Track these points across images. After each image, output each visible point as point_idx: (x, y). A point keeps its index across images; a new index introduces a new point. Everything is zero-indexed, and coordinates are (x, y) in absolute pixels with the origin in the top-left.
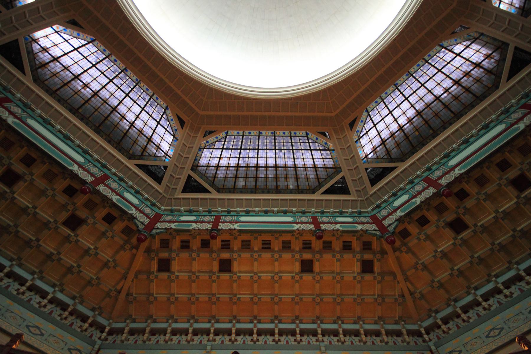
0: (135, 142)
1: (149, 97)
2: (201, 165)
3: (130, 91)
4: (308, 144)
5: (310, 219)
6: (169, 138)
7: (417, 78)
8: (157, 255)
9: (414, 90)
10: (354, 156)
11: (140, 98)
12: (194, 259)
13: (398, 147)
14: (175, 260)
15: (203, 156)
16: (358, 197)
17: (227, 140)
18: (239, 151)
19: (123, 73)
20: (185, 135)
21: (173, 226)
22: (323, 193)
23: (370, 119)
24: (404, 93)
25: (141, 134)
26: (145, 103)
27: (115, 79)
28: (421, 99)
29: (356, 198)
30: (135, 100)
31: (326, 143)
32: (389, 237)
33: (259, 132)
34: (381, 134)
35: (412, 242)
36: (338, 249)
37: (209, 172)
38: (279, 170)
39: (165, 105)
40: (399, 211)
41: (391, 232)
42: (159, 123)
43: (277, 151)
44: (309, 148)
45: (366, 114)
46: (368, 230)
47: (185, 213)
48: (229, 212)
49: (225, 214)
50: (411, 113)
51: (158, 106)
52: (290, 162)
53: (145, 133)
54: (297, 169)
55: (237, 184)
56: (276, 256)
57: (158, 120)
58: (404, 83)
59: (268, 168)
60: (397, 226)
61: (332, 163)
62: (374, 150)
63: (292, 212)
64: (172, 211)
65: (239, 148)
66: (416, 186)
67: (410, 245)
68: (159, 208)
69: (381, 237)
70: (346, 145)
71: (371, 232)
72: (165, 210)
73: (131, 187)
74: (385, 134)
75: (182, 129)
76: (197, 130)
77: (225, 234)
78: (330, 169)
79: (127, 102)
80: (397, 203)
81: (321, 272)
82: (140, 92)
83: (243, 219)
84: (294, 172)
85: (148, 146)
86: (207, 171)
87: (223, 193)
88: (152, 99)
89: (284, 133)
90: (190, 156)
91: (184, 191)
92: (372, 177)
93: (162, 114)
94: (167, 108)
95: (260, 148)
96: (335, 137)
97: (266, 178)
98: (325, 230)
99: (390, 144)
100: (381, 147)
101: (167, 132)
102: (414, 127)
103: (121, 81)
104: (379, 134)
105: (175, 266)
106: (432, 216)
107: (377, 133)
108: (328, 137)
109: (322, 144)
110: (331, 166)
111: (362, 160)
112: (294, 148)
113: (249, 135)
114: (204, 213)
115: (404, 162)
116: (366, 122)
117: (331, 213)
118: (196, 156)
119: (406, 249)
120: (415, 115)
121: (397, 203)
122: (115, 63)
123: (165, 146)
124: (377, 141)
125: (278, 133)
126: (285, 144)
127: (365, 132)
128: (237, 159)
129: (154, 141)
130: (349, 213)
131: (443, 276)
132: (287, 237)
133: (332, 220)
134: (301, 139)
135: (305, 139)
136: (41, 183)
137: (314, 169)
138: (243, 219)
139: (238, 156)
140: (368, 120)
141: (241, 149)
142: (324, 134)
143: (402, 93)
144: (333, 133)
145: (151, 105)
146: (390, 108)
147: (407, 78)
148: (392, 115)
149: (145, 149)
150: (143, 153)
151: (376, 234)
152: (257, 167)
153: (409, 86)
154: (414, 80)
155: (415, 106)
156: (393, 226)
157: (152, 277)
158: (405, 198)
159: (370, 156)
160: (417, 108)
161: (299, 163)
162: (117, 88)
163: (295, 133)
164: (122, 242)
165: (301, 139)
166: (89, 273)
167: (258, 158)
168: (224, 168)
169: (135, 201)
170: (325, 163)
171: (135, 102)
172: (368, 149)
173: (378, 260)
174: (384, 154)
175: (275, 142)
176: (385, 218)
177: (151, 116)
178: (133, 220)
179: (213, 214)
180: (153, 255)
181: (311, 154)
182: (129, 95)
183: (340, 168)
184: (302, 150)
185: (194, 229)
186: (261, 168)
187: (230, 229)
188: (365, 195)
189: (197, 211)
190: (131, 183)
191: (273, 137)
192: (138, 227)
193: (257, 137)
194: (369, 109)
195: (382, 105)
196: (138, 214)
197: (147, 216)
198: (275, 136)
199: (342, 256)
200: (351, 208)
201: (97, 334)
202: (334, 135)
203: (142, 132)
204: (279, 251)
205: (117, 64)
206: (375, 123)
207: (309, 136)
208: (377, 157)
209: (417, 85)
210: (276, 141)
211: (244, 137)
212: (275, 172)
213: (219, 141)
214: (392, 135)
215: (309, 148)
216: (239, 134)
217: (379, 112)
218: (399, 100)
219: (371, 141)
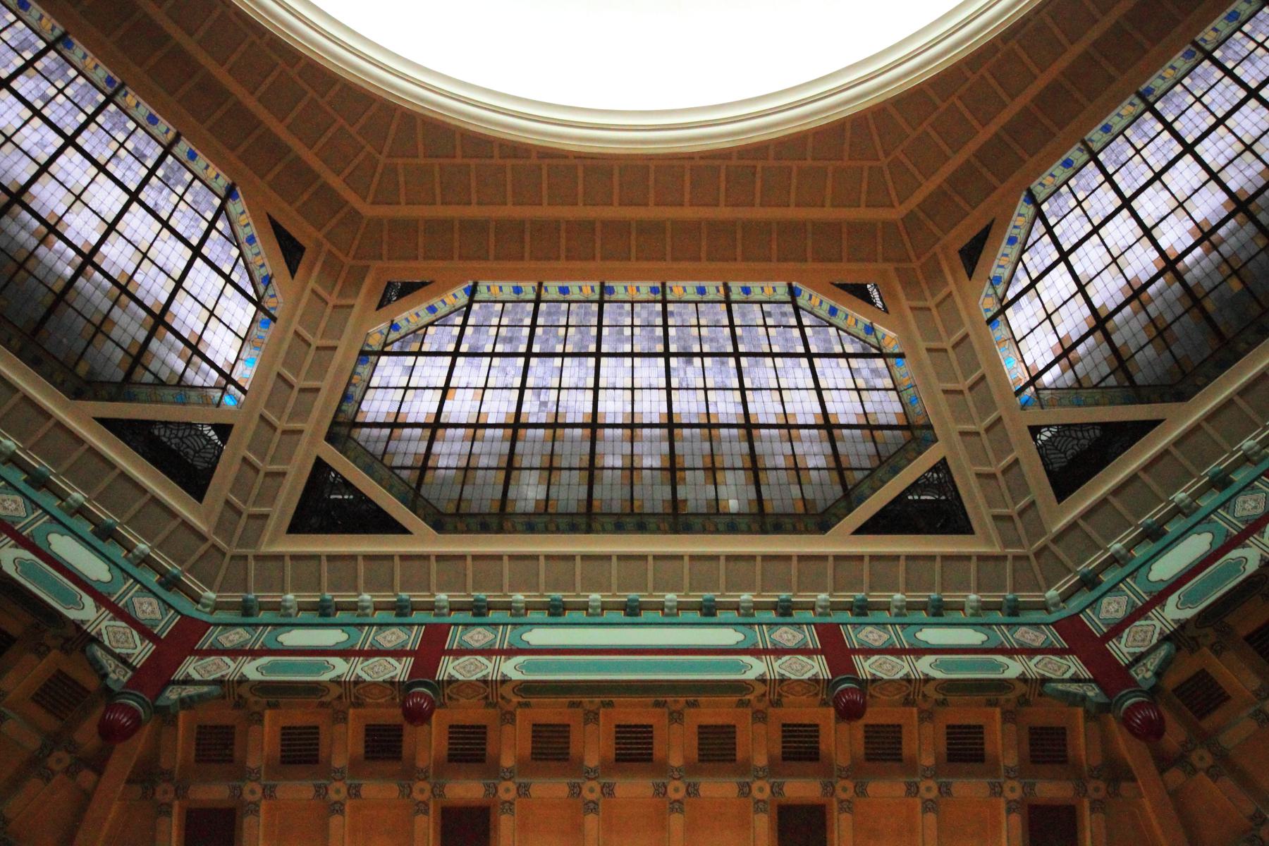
0: (98, 329)
1: (160, 150)
2: (369, 420)
3: (82, 128)
4: (796, 332)
5: (810, 638)
6: (240, 312)
7: (1229, 65)
8: (181, 792)
9: (1220, 114)
10: (983, 378)
11: (122, 152)
12: (337, 808)
13: (1159, 340)
14: (256, 812)
15: (374, 383)
16: (1006, 544)
17: (471, 321)
18: (521, 361)
19: (52, 54)
20: (304, 300)
21: (252, 670)
22: (861, 530)
23: (1043, 230)
24: (1177, 126)
25: (124, 298)
26: (144, 172)
27: (21, 78)
28: (1248, 148)
29: (997, 550)
30: (102, 162)
31: (870, 329)
32: (1136, 706)
33: (602, 285)
34: (1090, 290)
36: (927, 760)
37: (402, 446)
38: (683, 439)
39: (222, 183)
40: (1173, 600)
41: (1146, 687)
42: (197, 252)
43: (674, 362)
44: (801, 349)
45: (1029, 210)
46: (1050, 680)
47: (303, 617)
48: (479, 609)
49: (467, 617)
50: (1210, 204)
51: (196, 183)
52: (726, 407)
53: (140, 294)
54: (755, 432)
55: (512, 494)
56: (676, 789)
57: (195, 242)
58: (1178, 88)
59: (638, 431)
60: (1166, 664)
61: (898, 408)
62: (1065, 352)
63: (736, 607)
64: (246, 609)
65: (522, 348)
66: (1240, 499)
67: (1230, 739)
68: (196, 599)
69: (1105, 708)
70: (950, 333)
71: (1060, 686)
72: (218, 606)
73: (81, 511)
74: (1107, 292)
75: (293, 272)
76: (355, 279)
77: (462, 701)
78: (887, 433)
79: (69, 167)
80: (1166, 568)
82: (124, 128)
83: (538, 637)
84: (745, 446)
85: (154, 344)
86: (392, 444)
87: (456, 531)
88: (170, 159)
89: (702, 291)
90: (325, 385)
91: (298, 526)
92: (1059, 462)
93: (209, 216)
94: (230, 193)
95: (605, 349)
96: (905, 304)
97: (632, 469)
98: (875, 680)
99: (1128, 326)
100: (1091, 340)
101: (229, 288)
102: (1225, 260)
103: (44, 85)
104: (1081, 289)
107: (1073, 288)
108: (879, 304)
109: (852, 330)
110: (894, 421)
111: (1019, 392)
112: (742, 349)
113: (561, 297)
114: (379, 616)
115: (1189, 398)
116: (1030, 242)
117: (894, 611)
118: (349, 383)
119: (1209, 760)
120: (1225, 213)
121: (1166, 568)
122: (21, 12)
123: (221, 346)
124: (1074, 320)
125: (677, 289)
126: (704, 331)
127: (1025, 282)
128: (515, 395)
129: (175, 325)
130: (969, 611)
132: (713, 713)
133: (902, 638)
134: (770, 314)
135: (784, 314)
137: (824, 432)
138: (538, 637)
139: (517, 383)
140: (1035, 235)
141: (528, 355)
142: (859, 292)
143: (1168, 126)
144: (899, 288)
145: (165, 182)
146: (1122, 186)
147: (1187, 66)
148: (1134, 214)
149: (139, 356)
150: (129, 374)
151: (1084, 698)
152: (594, 425)
153: (1198, 99)
154: (1219, 74)
155: (1222, 176)
156: (1152, 663)
158: (1196, 545)
159: (1047, 379)
160: (1233, 186)
161: (764, 407)
162: (27, 113)
163: (746, 291)
164: (33, 743)
165: (770, 314)
167: (596, 389)
168: (461, 431)
169: (94, 568)
170: (869, 408)
171: (102, 168)
172: (1039, 350)
173: (1097, 806)
174: (1105, 370)
175: (665, 326)
176: (1117, 630)
177: (165, 224)
178: (83, 651)
179: (417, 617)
180: (164, 792)
181: (809, 372)
182: (79, 140)
183: (929, 427)
184: (773, 355)
185: (337, 682)
186: (608, 432)
187: (485, 681)
188: (1033, 537)
189: (353, 607)
190: (78, 496)
191: (659, 307)
192: (105, 676)
193: (595, 307)
194: (1040, 193)
195: (1092, 175)
196: (105, 623)
197: (146, 632)
198: (665, 302)
199: (945, 790)
200: (978, 590)
202: (901, 295)
203: (130, 288)
204: (690, 769)
205: (27, 18)
206: (1066, 247)
207: (802, 301)
208: (1078, 380)
209: (1228, 95)
210: (671, 321)
211: (543, 306)
212: (665, 446)
213: (442, 321)
214: (1136, 293)
215: (801, 349)
216: (522, 296)
217: (1079, 203)
218: (1159, 155)
219: (1049, 317)
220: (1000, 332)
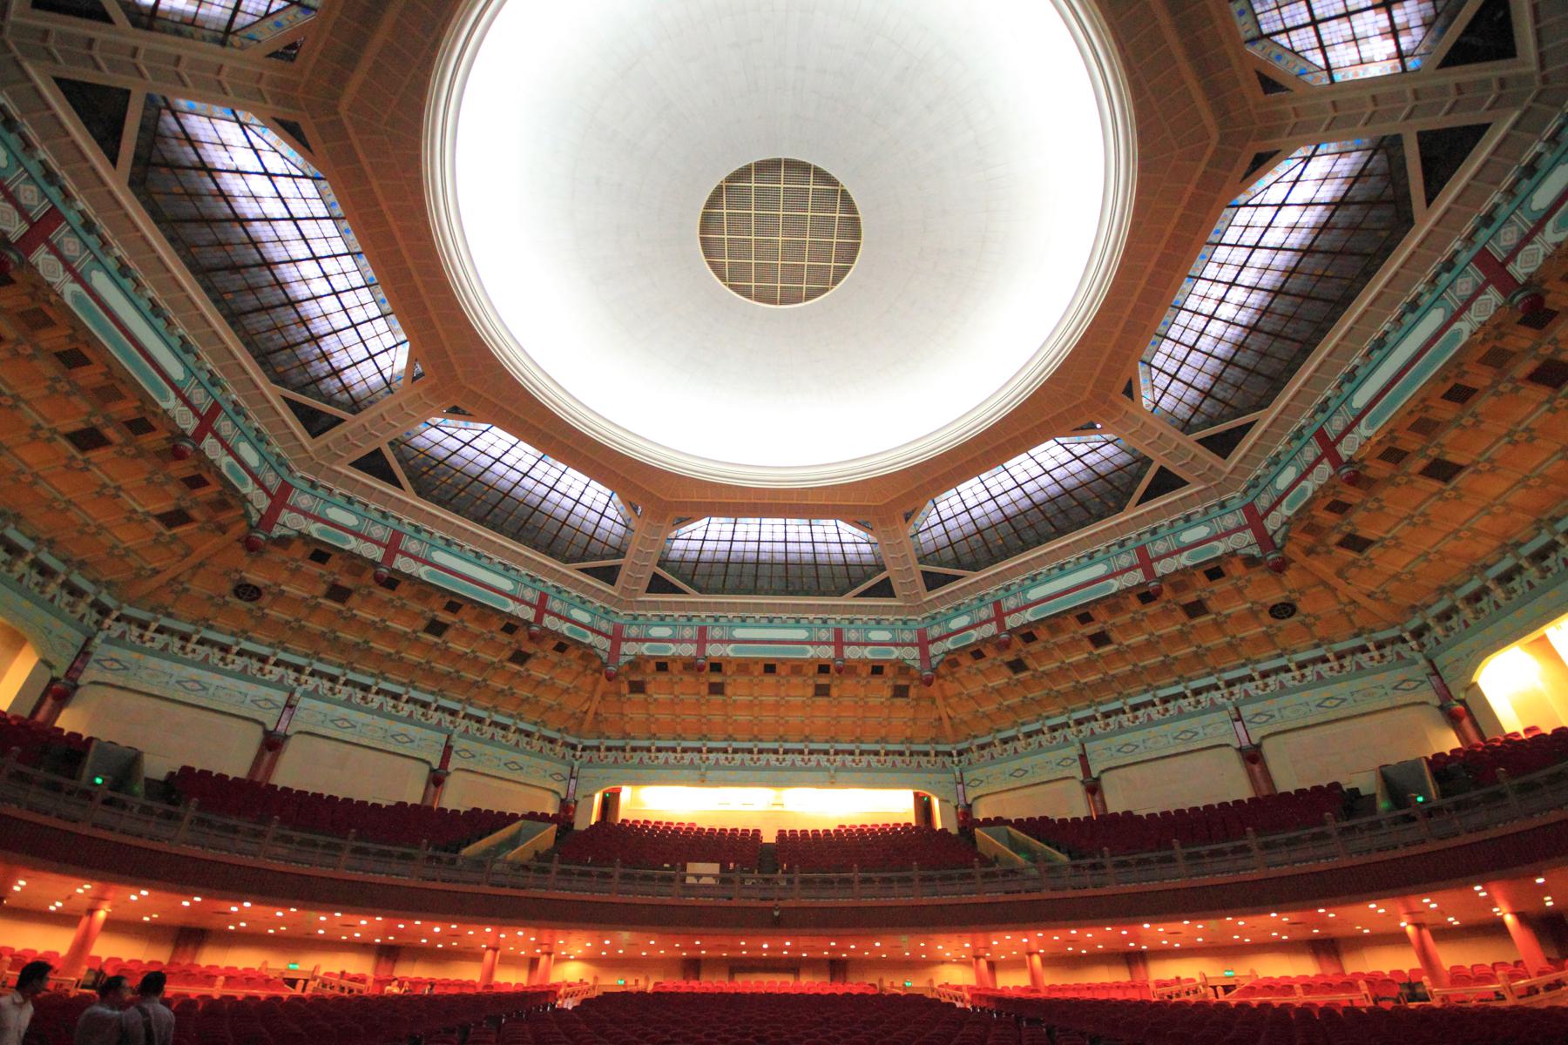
35: (961, 673)
36: (864, 675)
81: (840, 696)
91: (649, 591)
105: (651, 688)
106: (989, 652)
131: (990, 708)
136: (473, 627)
157: (623, 699)
166: (547, 699)
201: (569, 752)
220: (916, 540)
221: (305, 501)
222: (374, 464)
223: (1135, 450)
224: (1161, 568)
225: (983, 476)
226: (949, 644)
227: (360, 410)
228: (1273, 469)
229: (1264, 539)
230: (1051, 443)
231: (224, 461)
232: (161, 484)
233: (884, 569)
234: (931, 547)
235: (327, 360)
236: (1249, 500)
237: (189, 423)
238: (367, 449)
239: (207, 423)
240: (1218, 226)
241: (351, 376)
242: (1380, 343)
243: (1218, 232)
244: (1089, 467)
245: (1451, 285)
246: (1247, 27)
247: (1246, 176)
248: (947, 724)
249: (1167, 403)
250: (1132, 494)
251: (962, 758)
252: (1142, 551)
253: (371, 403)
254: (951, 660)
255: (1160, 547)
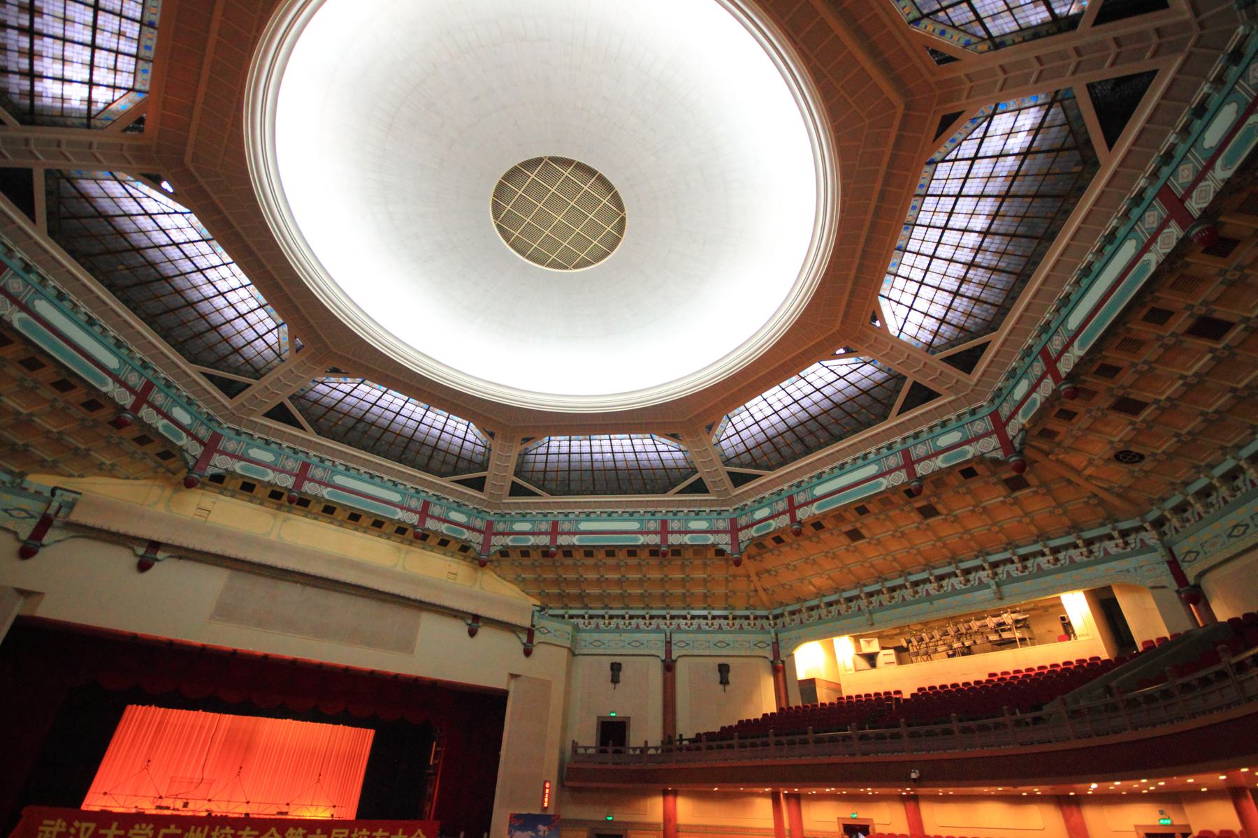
220: (718, 448)
221: (231, 446)
222: (280, 413)
223: (890, 370)
224: (921, 469)
225: (765, 395)
226: (753, 532)
227: (262, 376)
228: (1012, 382)
229: (1006, 443)
230: (816, 366)
231: (160, 424)
232: (118, 444)
233: (695, 471)
234: (730, 452)
235: (228, 342)
236: (994, 408)
237: (127, 400)
238: (271, 404)
239: (142, 396)
240: (922, 181)
241: (249, 352)
242: (1087, 271)
243: (922, 186)
244: (827, 397)
245: (1140, 218)
246: (907, 10)
247: (938, 136)
248: (761, 593)
249: (910, 329)
250: (892, 405)
251: (778, 621)
252: (906, 453)
253: (270, 370)
254: (758, 544)
255: (920, 451)
